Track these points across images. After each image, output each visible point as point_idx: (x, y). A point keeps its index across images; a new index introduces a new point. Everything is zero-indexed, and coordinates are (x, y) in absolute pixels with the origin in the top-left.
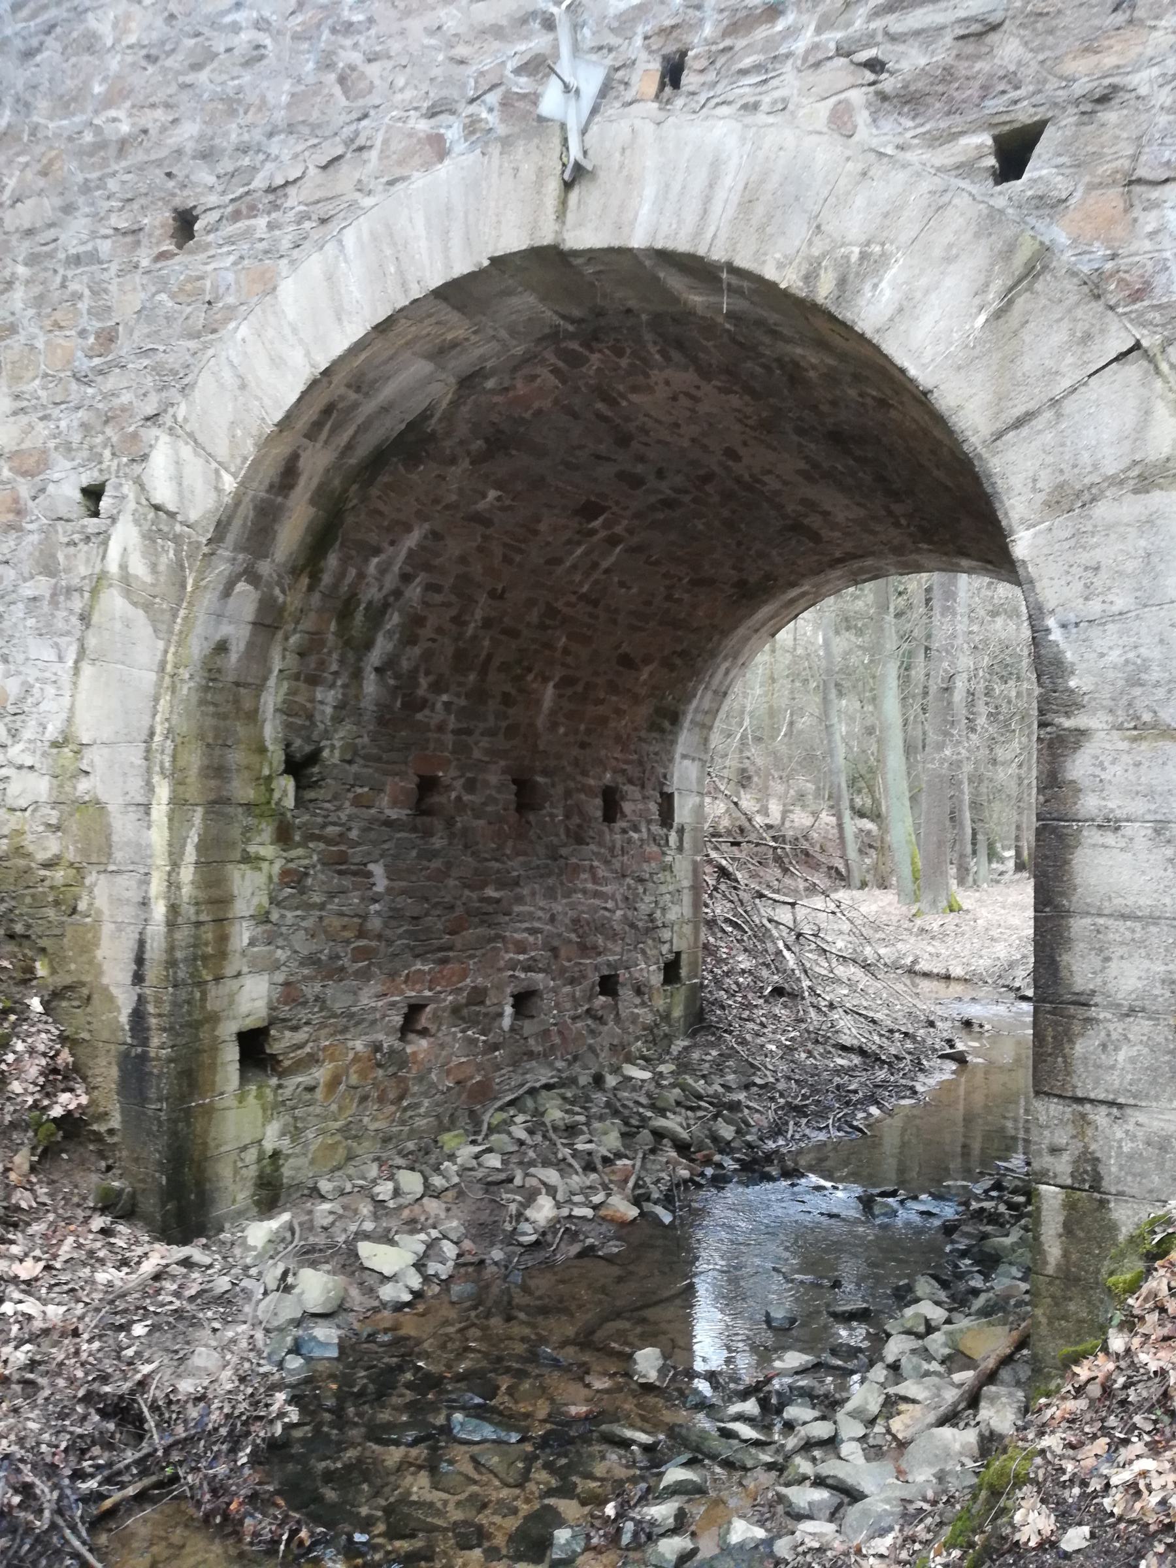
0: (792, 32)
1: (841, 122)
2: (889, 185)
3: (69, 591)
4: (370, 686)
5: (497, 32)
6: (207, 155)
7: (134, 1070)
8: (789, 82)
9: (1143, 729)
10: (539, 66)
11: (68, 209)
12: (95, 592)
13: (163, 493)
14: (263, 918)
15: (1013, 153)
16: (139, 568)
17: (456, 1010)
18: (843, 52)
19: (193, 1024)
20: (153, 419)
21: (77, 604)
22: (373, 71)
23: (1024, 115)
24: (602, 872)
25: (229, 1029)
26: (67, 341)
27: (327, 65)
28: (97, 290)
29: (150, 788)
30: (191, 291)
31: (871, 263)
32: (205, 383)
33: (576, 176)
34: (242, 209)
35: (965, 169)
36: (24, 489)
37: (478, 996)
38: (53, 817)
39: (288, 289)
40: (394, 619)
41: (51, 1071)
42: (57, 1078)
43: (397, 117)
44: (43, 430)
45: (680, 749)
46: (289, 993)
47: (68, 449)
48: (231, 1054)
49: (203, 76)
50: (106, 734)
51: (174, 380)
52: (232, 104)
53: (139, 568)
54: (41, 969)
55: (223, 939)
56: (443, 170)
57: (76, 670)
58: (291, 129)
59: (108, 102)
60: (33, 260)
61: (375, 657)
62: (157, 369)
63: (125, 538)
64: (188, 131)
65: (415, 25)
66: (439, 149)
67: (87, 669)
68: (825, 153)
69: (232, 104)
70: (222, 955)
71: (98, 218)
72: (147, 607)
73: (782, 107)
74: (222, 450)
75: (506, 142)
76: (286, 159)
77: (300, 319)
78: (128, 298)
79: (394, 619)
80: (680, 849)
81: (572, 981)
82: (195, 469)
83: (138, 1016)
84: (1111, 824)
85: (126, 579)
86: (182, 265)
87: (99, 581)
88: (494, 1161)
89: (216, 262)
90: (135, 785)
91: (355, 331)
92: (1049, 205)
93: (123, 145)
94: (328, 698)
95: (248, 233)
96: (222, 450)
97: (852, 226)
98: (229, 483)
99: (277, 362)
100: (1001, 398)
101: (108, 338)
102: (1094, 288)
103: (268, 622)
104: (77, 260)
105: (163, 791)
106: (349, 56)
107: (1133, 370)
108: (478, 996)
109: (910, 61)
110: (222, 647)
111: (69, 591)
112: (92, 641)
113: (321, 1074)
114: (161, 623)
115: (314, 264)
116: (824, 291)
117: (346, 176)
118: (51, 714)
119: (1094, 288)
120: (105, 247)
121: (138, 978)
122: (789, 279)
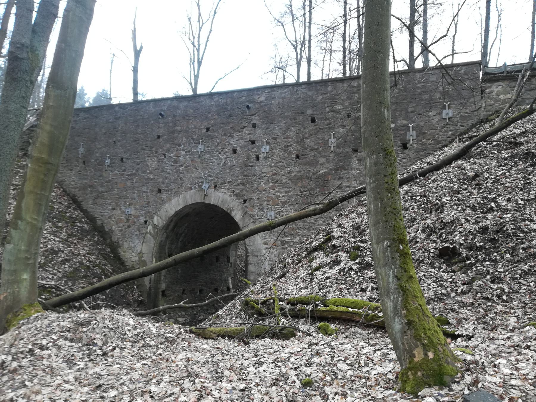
0: (226, 186)
1: (230, 195)
2: (234, 203)
3: (142, 234)
4: (179, 244)
5: (198, 178)
6: (163, 183)
7: (149, 294)
8: (226, 191)
9: (254, 256)
10: (202, 183)
11: (143, 185)
12: (146, 234)
13: (156, 223)
14: (165, 276)
15: (245, 201)
16: (152, 232)
17: (190, 291)
18: (231, 189)
19: (157, 289)
20: (155, 214)
21: (143, 235)
22: (184, 178)
23: (246, 198)
24: (215, 271)
25: (161, 290)
26: (143, 202)
27: (178, 176)
28: (147, 196)
29: (153, 259)
30: (160, 199)
31: (233, 210)
32: (162, 210)
33: (205, 196)
34: (168, 190)
35: (241, 202)
36: (136, 220)
37: (194, 289)
38: (138, 262)
39: (173, 201)
40: (183, 234)
41: (138, 295)
42: (139, 296)
43: (187, 184)
44: (139, 213)
45: (231, 249)
46: (167, 286)
47: (142, 216)
48: (161, 293)
49: (163, 173)
50: (147, 252)
51: (158, 209)
52: (166, 178)
53: (152, 232)
54: (136, 283)
55: (160, 278)
56: (192, 191)
57: (142, 244)
58: (174, 183)
59: (149, 173)
60: (138, 191)
61: (180, 240)
62: (155, 208)
63: (150, 228)
64: (161, 180)
65: (189, 175)
66: (191, 189)
67: (144, 244)
68: (229, 198)
69: (166, 178)
70: (160, 280)
71: (148, 187)
72: (153, 237)
73: (225, 193)
74: (164, 218)
75: (198, 191)
76: (173, 186)
77: (174, 205)
78: (152, 199)
79: (183, 234)
80: (231, 267)
81: (210, 288)
82: (160, 220)
83: (150, 288)
84: (251, 264)
85: (150, 233)
86: (159, 195)
87: (146, 233)
88: (195, 312)
89: (164, 196)
90: (150, 259)
91: (180, 207)
92: (247, 207)
93: (152, 179)
94: (174, 246)
95: (168, 193)
96: (164, 218)
97: (231, 206)
98: (165, 222)
99: (171, 209)
100: (243, 224)
101: (148, 203)
102: (250, 215)
103: (167, 238)
104: (144, 192)
105: (154, 260)
106: (181, 176)
107: (253, 223)
108: (194, 289)
109: (237, 191)
110: (162, 241)
111: (142, 234)
112: (145, 240)
113: (171, 298)
114: (155, 239)
115: (176, 199)
116: (229, 211)
117: (180, 190)
118: (139, 249)
119: (250, 215)
120: (149, 191)
121: (150, 283)
122: (226, 210)
